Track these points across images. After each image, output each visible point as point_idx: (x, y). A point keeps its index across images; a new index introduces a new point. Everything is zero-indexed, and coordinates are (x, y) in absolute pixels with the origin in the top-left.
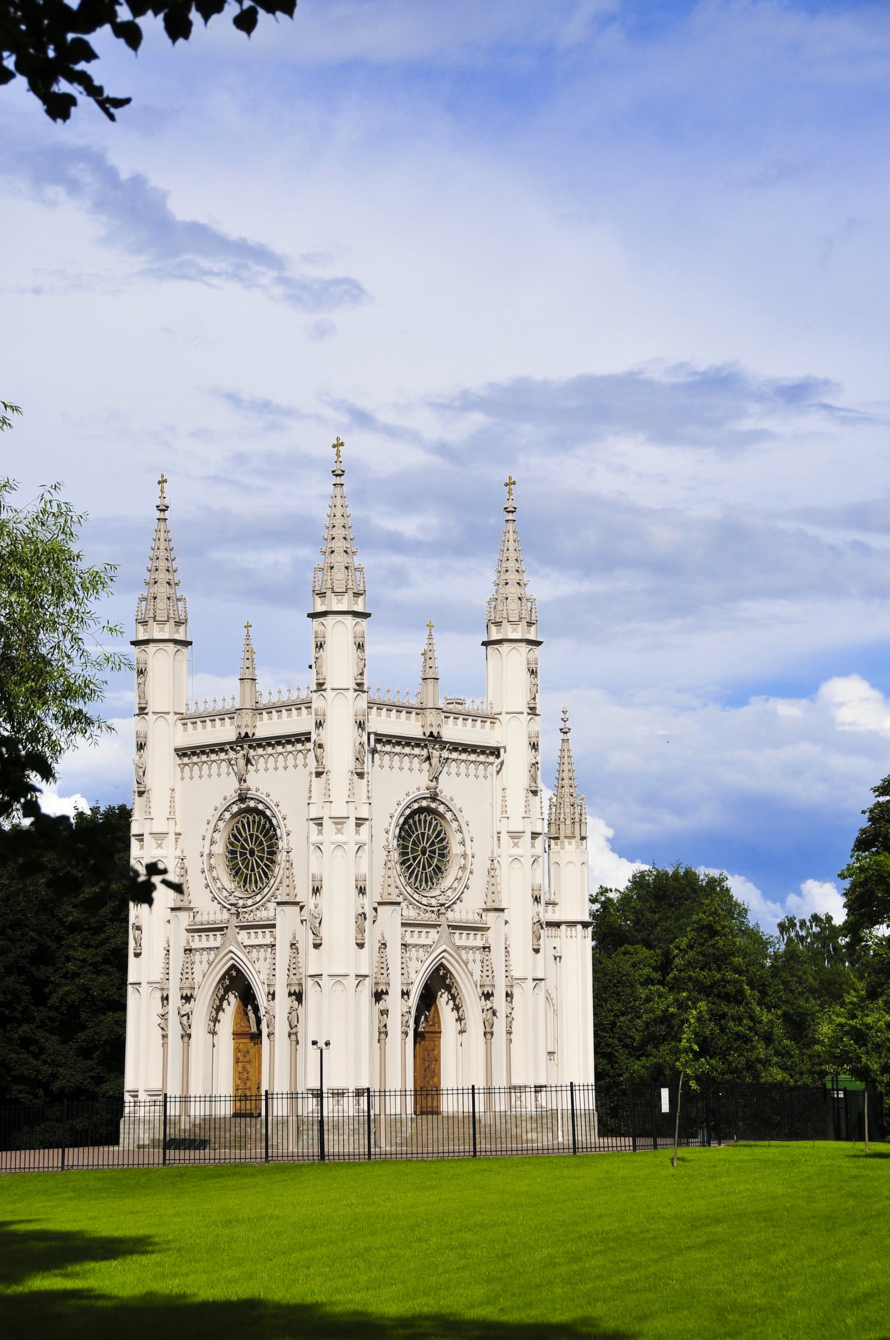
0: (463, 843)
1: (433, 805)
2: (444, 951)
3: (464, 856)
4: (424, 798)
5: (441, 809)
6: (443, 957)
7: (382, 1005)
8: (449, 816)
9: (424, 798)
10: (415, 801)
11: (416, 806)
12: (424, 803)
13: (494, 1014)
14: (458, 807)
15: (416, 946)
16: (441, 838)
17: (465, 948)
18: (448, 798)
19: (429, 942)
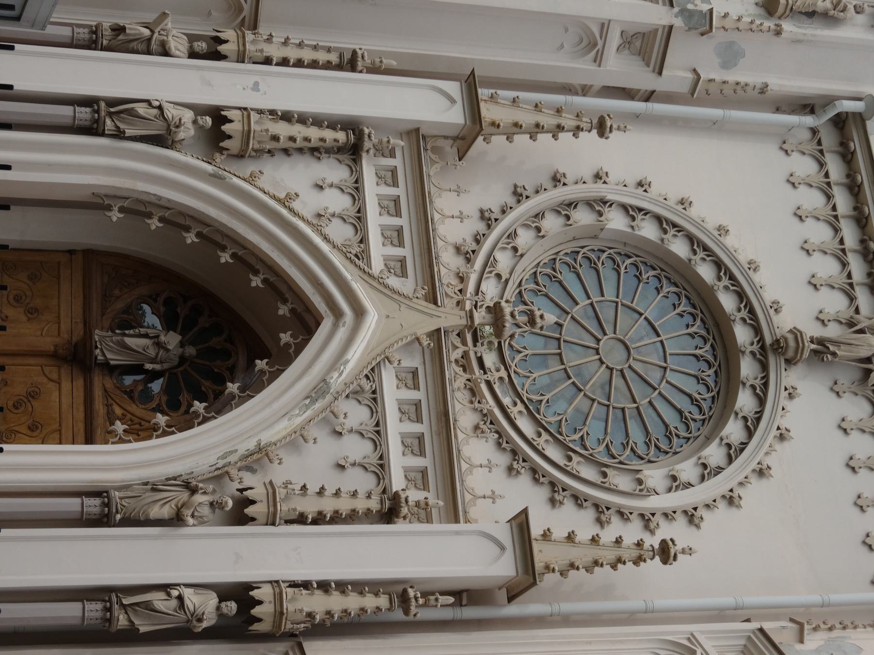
0: (675, 483)
1: (747, 368)
2: (360, 312)
3: (642, 489)
4: (757, 330)
5: (745, 401)
6: (338, 314)
7: (178, 44)
8: (733, 430)
9: (757, 330)
10: (741, 295)
11: (728, 302)
12: (742, 334)
13: (177, 520)
14: (768, 461)
15: (359, 220)
16: (665, 445)
17: (377, 434)
18: (784, 424)
19: (377, 266)
